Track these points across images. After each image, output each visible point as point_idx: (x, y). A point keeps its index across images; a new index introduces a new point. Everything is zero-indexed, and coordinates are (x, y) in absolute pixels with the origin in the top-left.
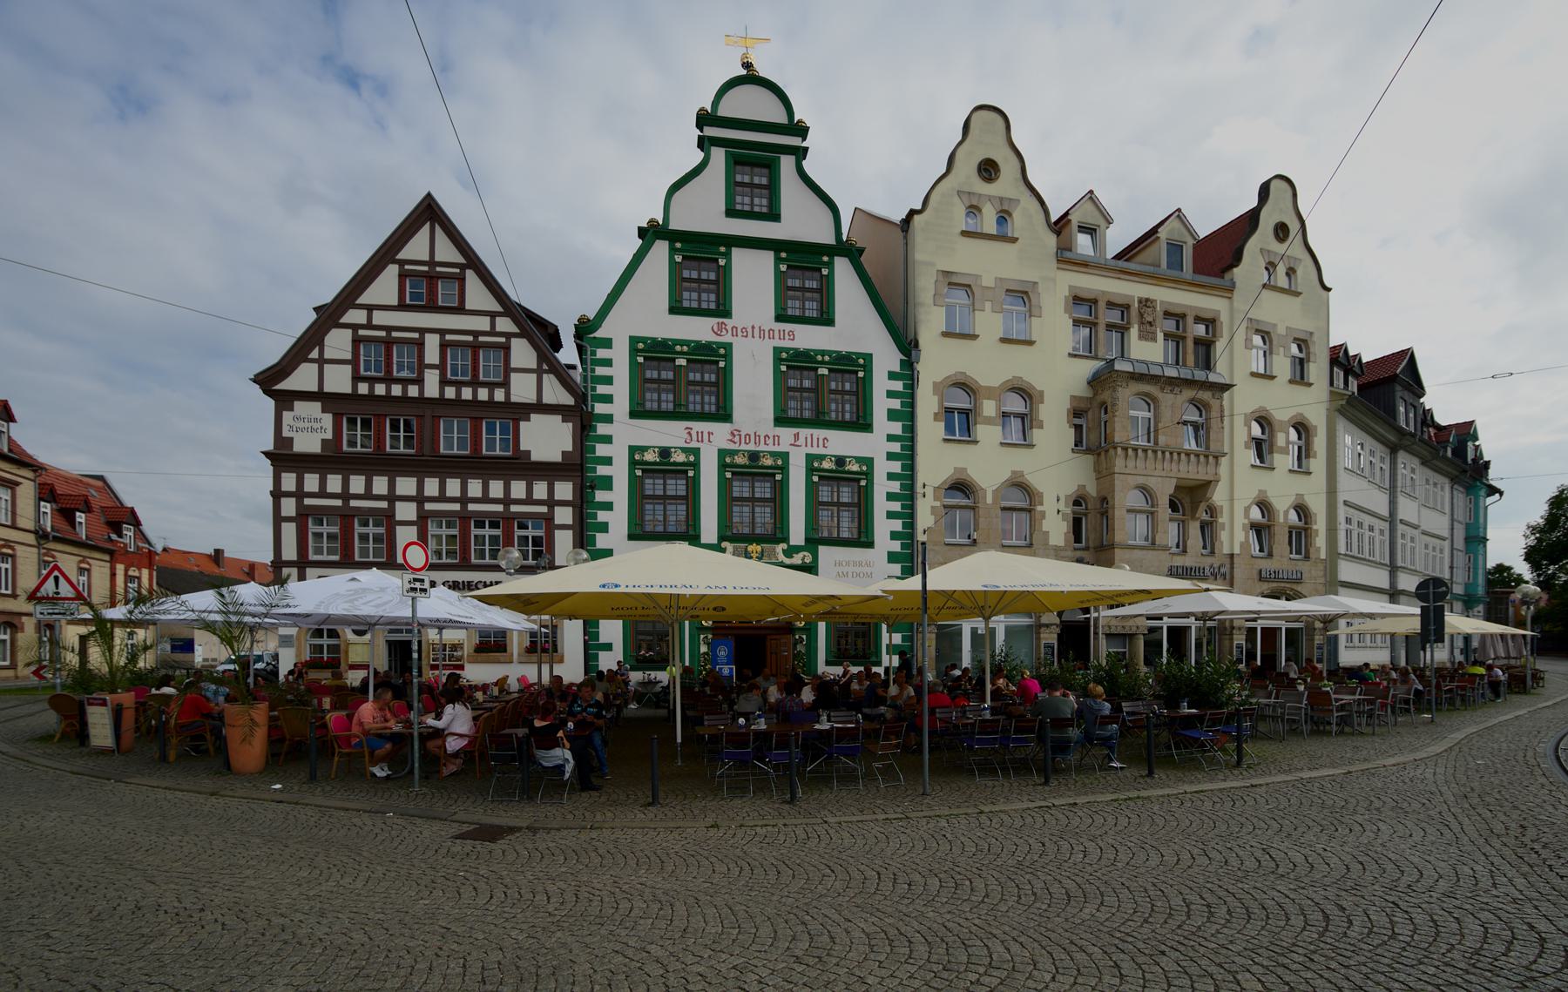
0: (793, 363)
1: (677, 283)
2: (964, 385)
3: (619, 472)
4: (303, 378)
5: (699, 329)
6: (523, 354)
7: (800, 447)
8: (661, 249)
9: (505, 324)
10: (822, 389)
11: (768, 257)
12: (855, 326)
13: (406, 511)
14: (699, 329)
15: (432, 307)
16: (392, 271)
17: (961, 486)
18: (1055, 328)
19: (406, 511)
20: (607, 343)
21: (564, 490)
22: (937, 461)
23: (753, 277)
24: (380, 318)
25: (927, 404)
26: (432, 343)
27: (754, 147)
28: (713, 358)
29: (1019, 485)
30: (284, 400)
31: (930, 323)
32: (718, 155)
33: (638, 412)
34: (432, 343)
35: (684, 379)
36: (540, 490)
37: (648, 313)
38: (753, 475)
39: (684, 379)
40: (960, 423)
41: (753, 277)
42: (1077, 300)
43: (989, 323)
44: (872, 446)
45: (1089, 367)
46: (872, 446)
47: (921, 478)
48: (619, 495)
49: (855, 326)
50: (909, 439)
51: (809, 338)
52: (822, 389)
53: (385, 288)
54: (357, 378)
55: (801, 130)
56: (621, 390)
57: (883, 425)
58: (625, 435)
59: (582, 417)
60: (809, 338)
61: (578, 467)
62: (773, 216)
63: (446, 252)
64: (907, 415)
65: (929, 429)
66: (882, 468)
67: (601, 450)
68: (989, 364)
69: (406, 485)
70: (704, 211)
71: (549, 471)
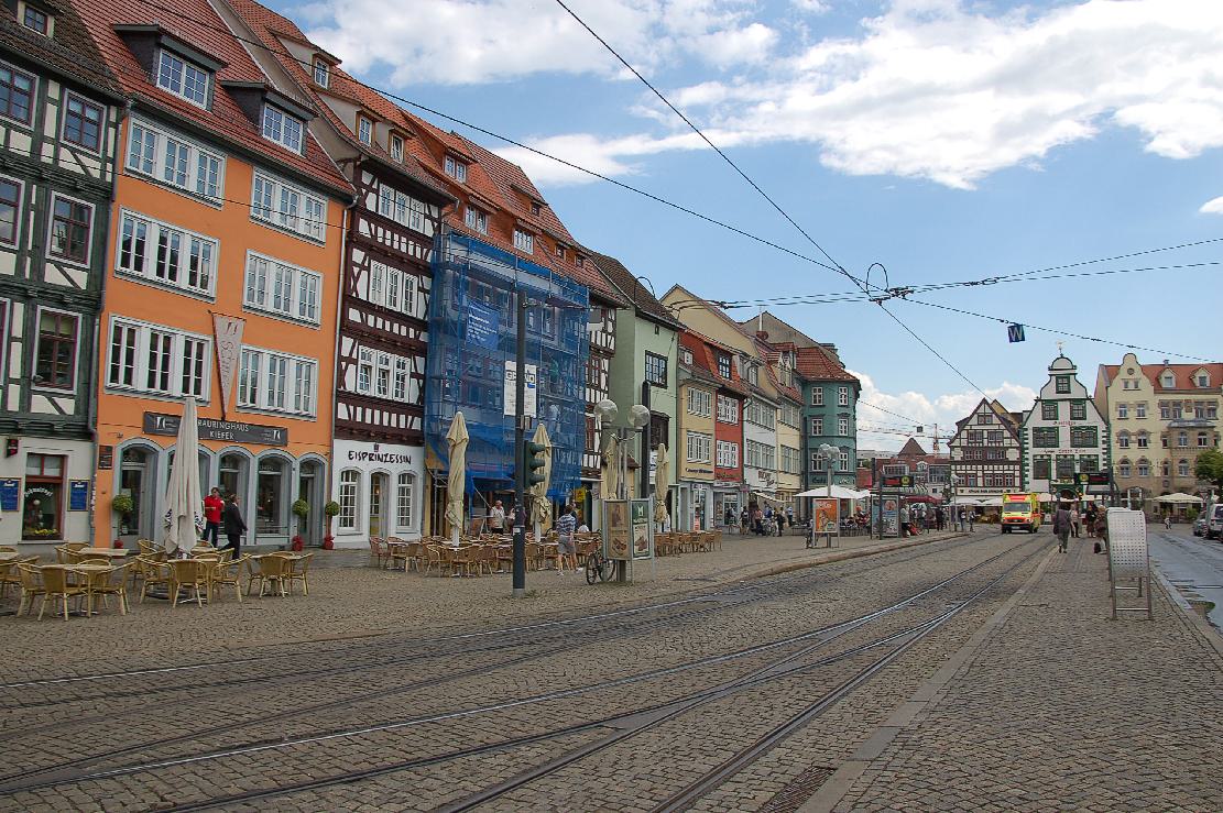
0: (1074, 430)
1: (1044, 411)
2: (1125, 433)
3: (1031, 462)
4: (956, 443)
5: (1050, 423)
6: (1007, 434)
7: (1077, 453)
8: (1040, 403)
9: (1002, 427)
10: (1084, 437)
11: (1068, 403)
12: (1092, 418)
13: (980, 474)
14: (1050, 423)
15: (985, 424)
16: (976, 416)
17: (1125, 461)
18: (1154, 412)
19: (980, 474)
20: (1026, 430)
21: (1017, 467)
22: (1117, 454)
23: (1064, 410)
24: (973, 427)
25: (1114, 438)
26: (985, 432)
27: (1063, 377)
28: (1054, 431)
29: (1143, 460)
30: (952, 448)
31: (1113, 415)
32: (1054, 378)
33: (1036, 445)
34: (985, 432)
35: (1046, 437)
36: (1012, 467)
37: (1036, 421)
38: (1065, 464)
39: (1046, 437)
40: (1125, 444)
41: (1064, 410)
42: (1162, 404)
43: (1132, 414)
44: (1099, 451)
45: (1166, 423)
46: (1099, 451)
47: (1113, 458)
48: (1030, 468)
49: (1092, 418)
50: (1108, 450)
51: (1078, 423)
52: (1084, 437)
53: (974, 421)
54: (968, 443)
55: (1074, 367)
56: (1030, 441)
57: (1101, 445)
58: (1033, 452)
59: (1022, 450)
60: (1078, 423)
61: (1021, 462)
62: (1069, 392)
63: (988, 410)
64: (1107, 442)
65: (1115, 446)
66: (1101, 457)
67: (1026, 456)
68: (1133, 425)
69: (980, 467)
70: (1051, 394)
71: (1013, 463)
